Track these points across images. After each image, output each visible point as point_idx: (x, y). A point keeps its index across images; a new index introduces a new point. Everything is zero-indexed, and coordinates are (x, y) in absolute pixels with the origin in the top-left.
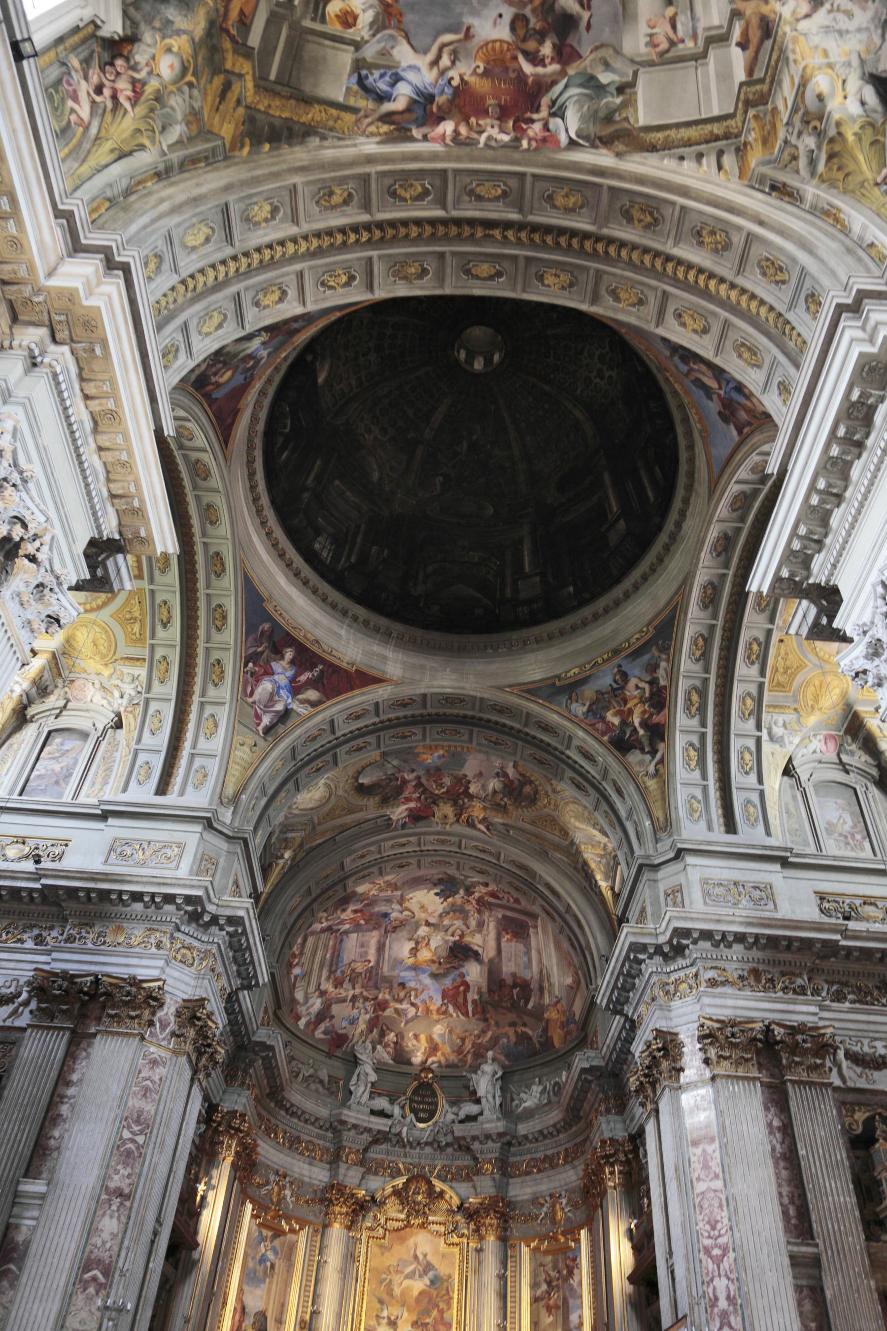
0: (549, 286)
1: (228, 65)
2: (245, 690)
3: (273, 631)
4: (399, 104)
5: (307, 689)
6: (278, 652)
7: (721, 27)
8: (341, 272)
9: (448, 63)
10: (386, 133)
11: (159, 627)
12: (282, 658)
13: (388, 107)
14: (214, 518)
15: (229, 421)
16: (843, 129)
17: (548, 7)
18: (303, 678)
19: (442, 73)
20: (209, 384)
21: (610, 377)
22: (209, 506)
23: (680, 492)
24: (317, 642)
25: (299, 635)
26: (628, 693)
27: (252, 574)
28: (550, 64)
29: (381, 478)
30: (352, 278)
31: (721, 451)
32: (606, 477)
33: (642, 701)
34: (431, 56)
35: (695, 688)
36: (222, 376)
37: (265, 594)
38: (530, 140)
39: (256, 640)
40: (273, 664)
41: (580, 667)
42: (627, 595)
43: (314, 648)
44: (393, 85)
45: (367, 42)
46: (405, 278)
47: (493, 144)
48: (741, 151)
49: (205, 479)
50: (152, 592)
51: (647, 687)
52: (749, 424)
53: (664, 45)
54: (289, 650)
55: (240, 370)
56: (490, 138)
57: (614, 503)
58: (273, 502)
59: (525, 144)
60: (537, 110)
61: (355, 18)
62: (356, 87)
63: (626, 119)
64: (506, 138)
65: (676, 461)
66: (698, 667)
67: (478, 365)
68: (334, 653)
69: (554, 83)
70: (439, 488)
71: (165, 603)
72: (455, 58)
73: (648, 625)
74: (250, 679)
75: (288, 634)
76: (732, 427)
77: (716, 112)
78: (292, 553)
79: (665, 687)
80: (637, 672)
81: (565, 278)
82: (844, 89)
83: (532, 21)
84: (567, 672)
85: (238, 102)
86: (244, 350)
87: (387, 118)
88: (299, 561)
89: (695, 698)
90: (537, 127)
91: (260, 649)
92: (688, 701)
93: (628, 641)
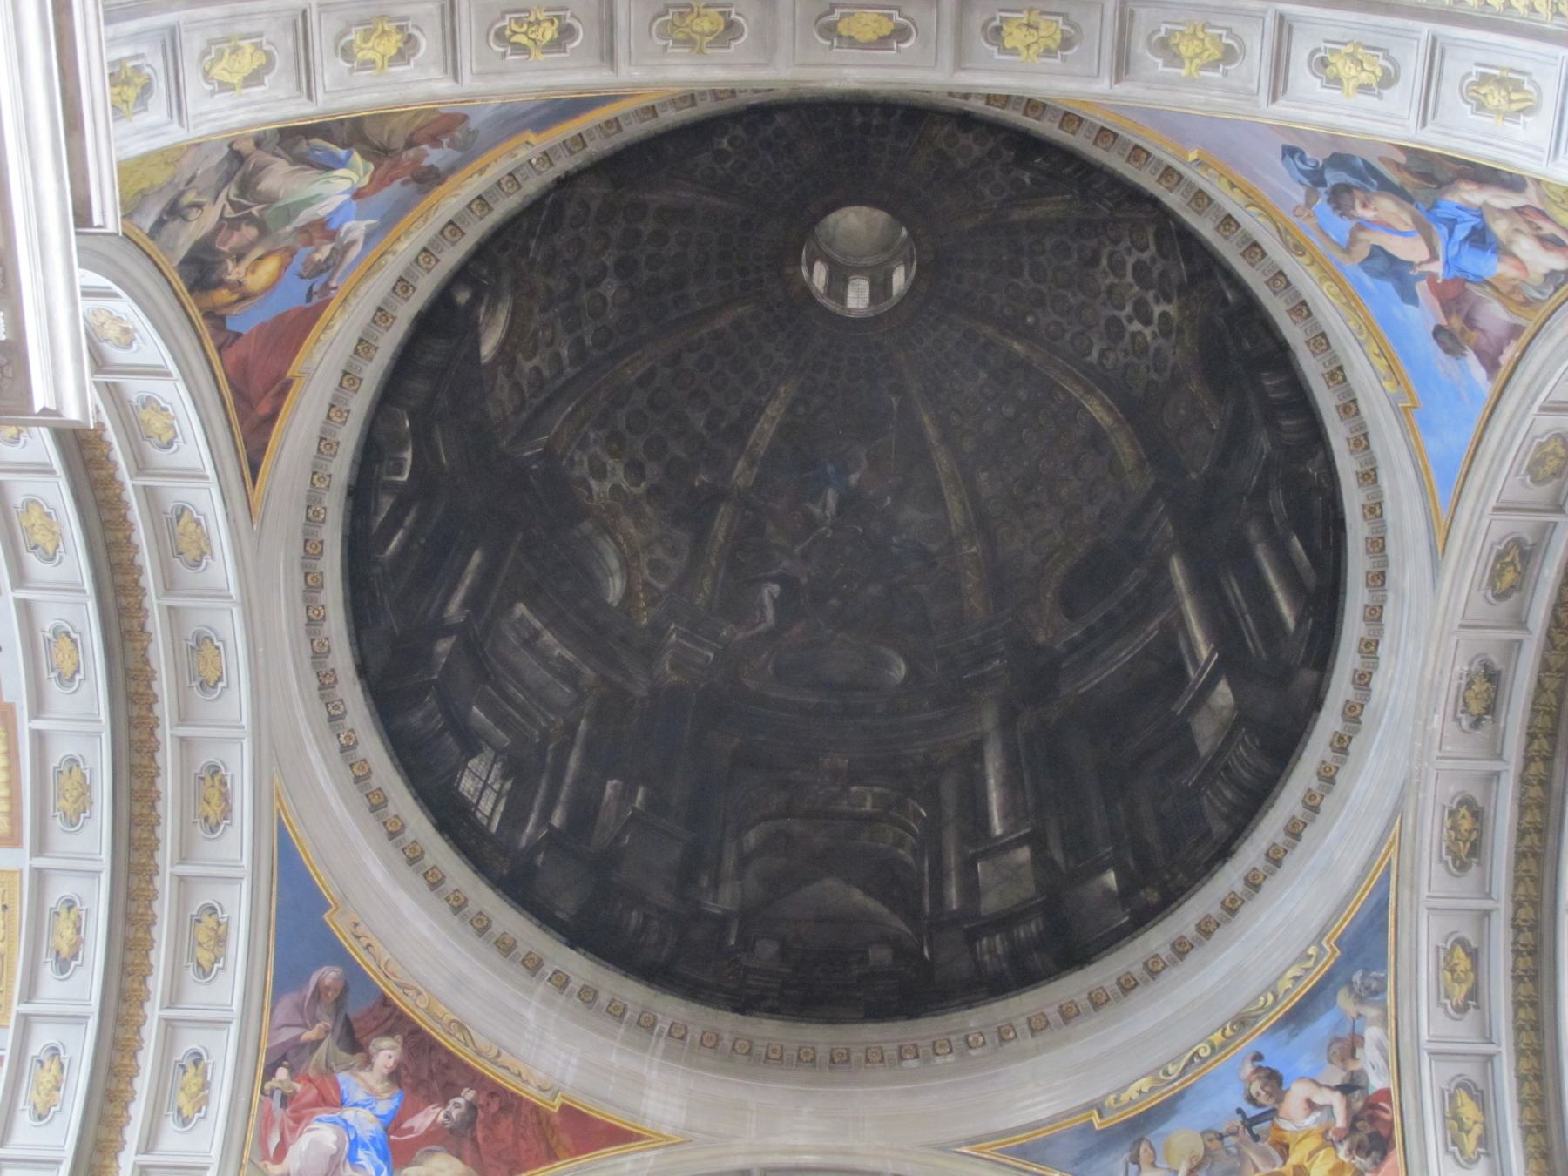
0: (1014, 51)
2: (263, 1140)
3: (345, 990)
5: (433, 1152)
6: (354, 1043)
8: (542, 15)
11: (48, 971)
12: (368, 1062)
14: (211, 675)
15: (264, 409)
18: (422, 1121)
20: (221, 283)
21: (1164, 315)
22: (202, 640)
23: (1356, 597)
24: (462, 1027)
25: (414, 1008)
26: (1287, 1126)
27: (297, 833)
29: (629, 593)
30: (566, 32)
31: (1453, 439)
32: (1177, 568)
33: (1328, 1140)
35: (1465, 1086)
36: (252, 270)
37: (329, 890)
39: (299, 1008)
40: (342, 1077)
41: (1152, 1073)
42: (1253, 884)
43: (452, 1044)
46: (688, 42)
49: (196, 564)
50: (40, 876)
51: (1337, 1100)
52: (1515, 331)
54: (386, 1042)
55: (297, 264)
57: (1199, 635)
58: (362, 670)
65: (1338, 524)
66: (1461, 1031)
67: (858, 297)
68: (506, 1058)
70: (770, 614)
71: (70, 904)
73: (1322, 934)
74: (279, 1113)
75: (385, 1001)
76: (1472, 359)
78: (403, 802)
79: (1385, 1094)
80: (1305, 1065)
81: (1051, 29)
84: (1124, 1088)
86: (308, 203)
88: (419, 825)
89: (1469, 1110)
91: (309, 1035)
92: (1453, 1121)
93: (1272, 987)
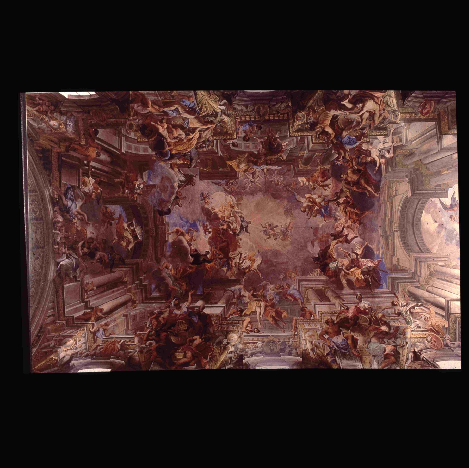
1: (61, 144)
4: (65, 202)
7: (89, 305)
9: (79, 218)
10: (55, 197)
13: (64, 198)
16: (54, 354)
17: (96, 249)
19: (76, 216)
28: (82, 252)
34: (80, 211)
38: (59, 248)
44: (70, 199)
45: (80, 190)
47: (55, 235)
48: (54, 322)
53: (86, 288)
56: (58, 234)
59: (57, 246)
60: (68, 250)
61: (86, 186)
62: (67, 187)
63: (66, 280)
64: (58, 240)
69: (76, 254)
72: (81, 220)
77: (66, 310)
82: (68, 350)
83: (92, 244)
85: (52, 146)
87: (60, 198)
90: (64, 250)
